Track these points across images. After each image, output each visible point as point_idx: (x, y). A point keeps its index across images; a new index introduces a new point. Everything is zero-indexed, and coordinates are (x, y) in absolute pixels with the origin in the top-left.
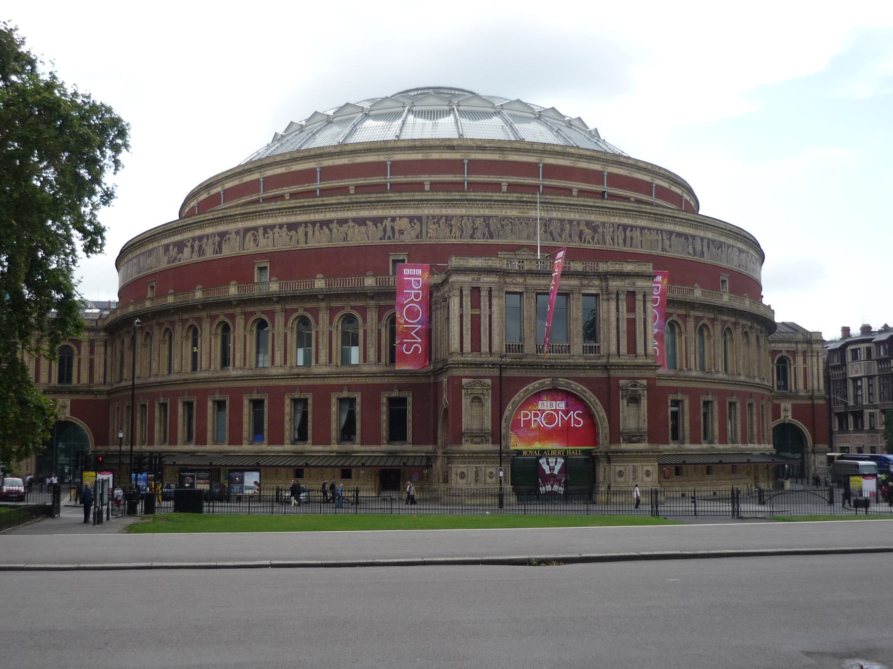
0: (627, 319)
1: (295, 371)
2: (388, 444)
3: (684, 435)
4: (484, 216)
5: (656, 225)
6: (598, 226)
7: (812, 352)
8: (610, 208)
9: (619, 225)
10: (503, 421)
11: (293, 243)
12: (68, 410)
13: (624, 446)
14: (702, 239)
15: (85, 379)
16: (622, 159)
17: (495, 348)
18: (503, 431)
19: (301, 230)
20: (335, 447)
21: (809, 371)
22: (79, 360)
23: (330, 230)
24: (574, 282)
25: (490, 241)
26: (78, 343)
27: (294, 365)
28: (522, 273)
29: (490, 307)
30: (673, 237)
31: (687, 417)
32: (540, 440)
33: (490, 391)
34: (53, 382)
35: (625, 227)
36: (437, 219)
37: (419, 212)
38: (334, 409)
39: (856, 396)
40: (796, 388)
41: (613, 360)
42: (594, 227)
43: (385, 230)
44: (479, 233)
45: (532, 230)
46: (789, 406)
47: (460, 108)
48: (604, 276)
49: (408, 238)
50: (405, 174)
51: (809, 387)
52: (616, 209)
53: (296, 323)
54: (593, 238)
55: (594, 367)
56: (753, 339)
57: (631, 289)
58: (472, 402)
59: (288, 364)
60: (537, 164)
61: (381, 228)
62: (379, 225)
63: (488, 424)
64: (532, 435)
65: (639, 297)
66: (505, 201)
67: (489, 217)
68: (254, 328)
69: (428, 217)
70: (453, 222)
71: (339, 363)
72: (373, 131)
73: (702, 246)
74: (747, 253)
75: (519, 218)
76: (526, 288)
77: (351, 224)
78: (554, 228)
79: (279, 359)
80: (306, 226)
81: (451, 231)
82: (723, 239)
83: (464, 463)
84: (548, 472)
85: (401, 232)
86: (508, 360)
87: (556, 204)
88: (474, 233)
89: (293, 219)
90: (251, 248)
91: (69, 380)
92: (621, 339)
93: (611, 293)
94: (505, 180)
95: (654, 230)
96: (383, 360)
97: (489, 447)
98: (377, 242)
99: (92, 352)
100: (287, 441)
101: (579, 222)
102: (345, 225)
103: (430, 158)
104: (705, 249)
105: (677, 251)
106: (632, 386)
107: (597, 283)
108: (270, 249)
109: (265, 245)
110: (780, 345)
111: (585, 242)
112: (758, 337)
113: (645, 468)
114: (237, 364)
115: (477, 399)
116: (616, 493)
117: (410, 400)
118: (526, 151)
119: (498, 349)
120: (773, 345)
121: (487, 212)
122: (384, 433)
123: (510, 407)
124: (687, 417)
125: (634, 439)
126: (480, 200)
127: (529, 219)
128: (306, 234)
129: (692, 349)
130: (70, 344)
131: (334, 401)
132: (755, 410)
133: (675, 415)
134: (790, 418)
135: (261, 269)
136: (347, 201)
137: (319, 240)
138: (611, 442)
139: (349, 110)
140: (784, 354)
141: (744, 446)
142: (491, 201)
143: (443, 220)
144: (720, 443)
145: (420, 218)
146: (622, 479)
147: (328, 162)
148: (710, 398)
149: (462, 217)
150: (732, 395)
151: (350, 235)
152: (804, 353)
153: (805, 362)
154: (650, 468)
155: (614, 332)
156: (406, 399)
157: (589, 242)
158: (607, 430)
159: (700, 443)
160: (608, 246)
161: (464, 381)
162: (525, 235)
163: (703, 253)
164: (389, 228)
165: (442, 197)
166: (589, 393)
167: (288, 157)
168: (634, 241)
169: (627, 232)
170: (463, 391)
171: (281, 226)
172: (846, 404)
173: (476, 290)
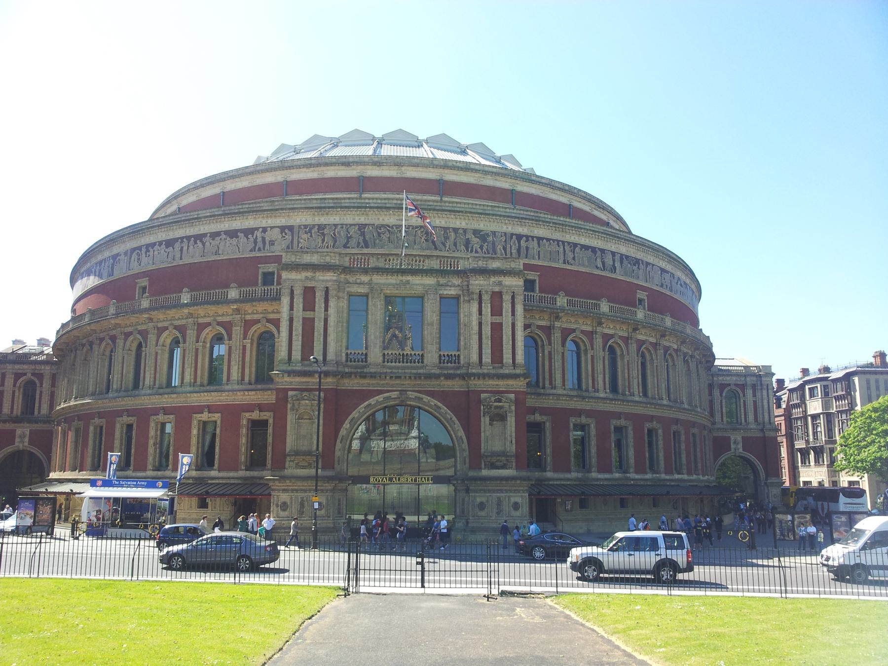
0: (492, 323)
2: (246, 470)
3: (590, 462)
5: (557, 236)
7: (761, 385)
8: (500, 216)
9: (512, 235)
11: (170, 259)
12: (27, 440)
13: (485, 472)
14: (613, 254)
15: (45, 410)
16: (533, 178)
17: (331, 356)
18: (338, 453)
19: (177, 246)
21: (759, 404)
22: (41, 392)
23: (204, 244)
24: (430, 281)
25: (365, 251)
26: (40, 376)
28: (365, 271)
29: (326, 309)
30: (577, 249)
31: (593, 443)
34: (15, 413)
35: (519, 237)
36: (308, 229)
37: (291, 222)
38: (195, 432)
39: (815, 433)
40: (746, 421)
42: (484, 235)
43: (255, 242)
44: (353, 242)
46: (739, 439)
49: (277, 250)
51: (760, 419)
52: (508, 217)
54: (481, 247)
56: (680, 362)
57: (497, 289)
58: (300, 418)
59: (157, 386)
60: (436, 180)
61: (252, 239)
62: (250, 236)
65: (507, 298)
66: (381, 208)
71: (206, 382)
73: (614, 261)
74: (673, 275)
76: (372, 289)
77: (223, 236)
80: (182, 242)
81: (323, 240)
82: (640, 255)
85: (272, 243)
86: (347, 370)
88: (348, 242)
89: (171, 235)
90: (136, 269)
91: (33, 413)
93: (473, 293)
95: (554, 241)
96: (247, 378)
97: (313, 472)
99: (53, 385)
100: (150, 467)
101: (465, 231)
102: (218, 238)
103: (326, 176)
104: (617, 264)
106: (496, 401)
107: (457, 281)
109: (147, 264)
110: (728, 378)
112: (686, 362)
113: (513, 500)
114: (115, 387)
116: (473, 531)
117: (271, 421)
118: (425, 166)
119: (334, 358)
120: (720, 378)
121: (362, 220)
122: (243, 459)
124: (593, 443)
126: (354, 207)
128: (181, 250)
129: (599, 367)
130: (32, 378)
132: (683, 438)
134: (741, 450)
135: (144, 288)
137: (193, 256)
138: (471, 468)
140: (733, 387)
141: (668, 477)
144: (636, 472)
145: (291, 228)
146: (483, 513)
147: (230, 186)
148: (622, 422)
149: (336, 225)
150: (652, 421)
151: (221, 248)
152: (754, 387)
153: (754, 395)
154: (519, 500)
155: (476, 338)
156: (267, 421)
157: (476, 252)
158: (466, 454)
161: (290, 393)
163: (615, 268)
164: (259, 240)
166: (444, 409)
168: (530, 251)
169: (522, 242)
170: (289, 406)
171: (160, 243)
172: (807, 442)
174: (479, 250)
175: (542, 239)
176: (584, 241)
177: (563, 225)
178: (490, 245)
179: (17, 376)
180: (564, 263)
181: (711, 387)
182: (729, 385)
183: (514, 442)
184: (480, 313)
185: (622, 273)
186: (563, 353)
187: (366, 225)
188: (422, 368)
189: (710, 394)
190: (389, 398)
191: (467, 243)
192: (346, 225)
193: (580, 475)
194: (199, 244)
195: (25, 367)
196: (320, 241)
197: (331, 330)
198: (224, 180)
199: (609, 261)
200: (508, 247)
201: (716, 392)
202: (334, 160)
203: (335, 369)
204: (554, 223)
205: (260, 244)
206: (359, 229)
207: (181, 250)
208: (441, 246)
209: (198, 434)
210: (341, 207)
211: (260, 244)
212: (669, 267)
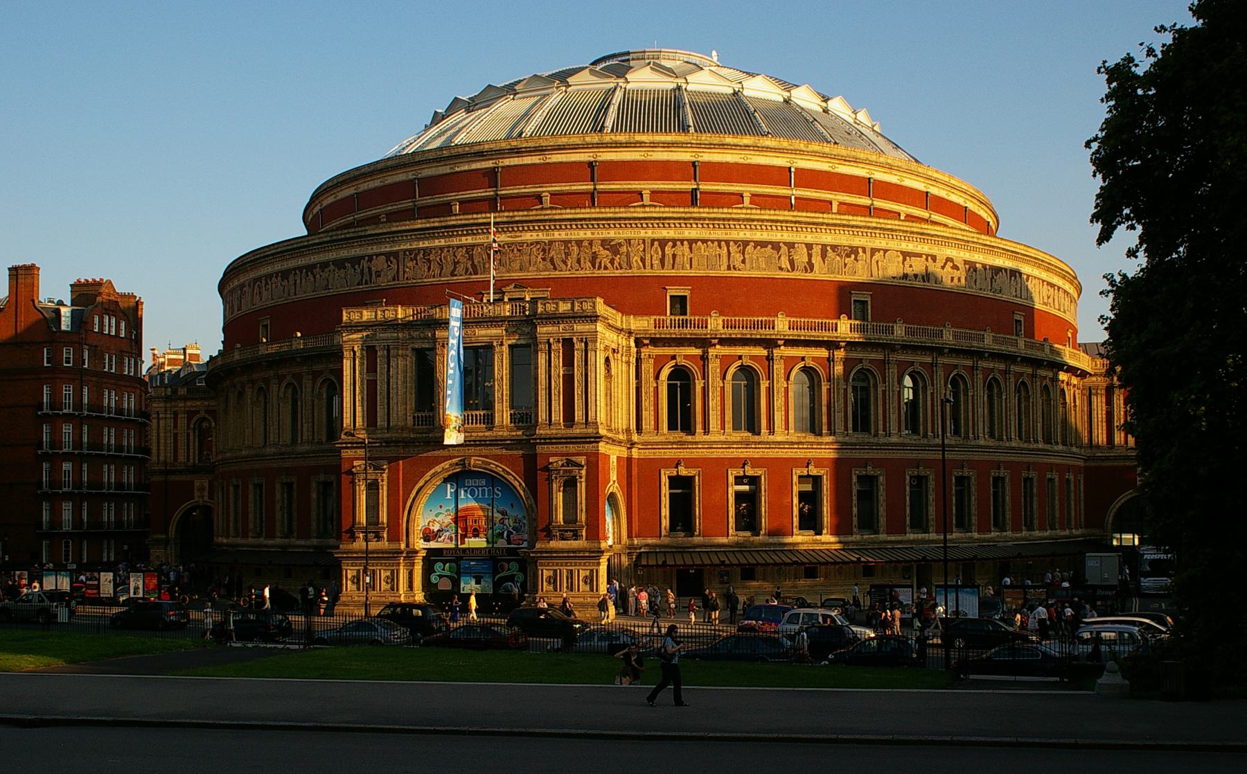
1: (283, 449)
6: (620, 245)
9: (653, 241)
13: (554, 544)
14: (809, 246)
19: (291, 278)
20: (315, 541)
30: (749, 248)
35: (663, 243)
38: (314, 495)
43: (362, 273)
44: (461, 268)
45: (526, 258)
49: (383, 282)
53: (290, 390)
54: (612, 262)
57: (567, 336)
60: (590, 164)
65: (579, 346)
67: (473, 246)
68: (262, 399)
71: (324, 439)
73: (810, 256)
74: (934, 258)
75: (509, 245)
77: (332, 267)
79: (273, 438)
81: (429, 268)
82: (858, 241)
88: (454, 270)
90: (259, 305)
94: (546, 190)
95: (713, 241)
98: (355, 288)
100: (278, 534)
101: (591, 243)
104: (816, 260)
105: (757, 268)
108: (270, 303)
111: (599, 268)
115: (373, 487)
131: (314, 485)
133: (739, 496)
145: (395, 254)
147: (365, 186)
149: (442, 248)
157: (606, 268)
160: (635, 272)
163: (810, 266)
164: (366, 270)
168: (678, 259)
171: (277, 274)
175: (696, 241)
178: (624, 258)
189: (1109, 402)
191: (594, 257)
194: (311, 277)
198: (356, 178)
199: (801, 257)
200: (648, 257)
204: (710, 219)
205: (367, 277)
206: (467, 252)
209: (318, 498)
211: (367, 277)
212: (924, 248)
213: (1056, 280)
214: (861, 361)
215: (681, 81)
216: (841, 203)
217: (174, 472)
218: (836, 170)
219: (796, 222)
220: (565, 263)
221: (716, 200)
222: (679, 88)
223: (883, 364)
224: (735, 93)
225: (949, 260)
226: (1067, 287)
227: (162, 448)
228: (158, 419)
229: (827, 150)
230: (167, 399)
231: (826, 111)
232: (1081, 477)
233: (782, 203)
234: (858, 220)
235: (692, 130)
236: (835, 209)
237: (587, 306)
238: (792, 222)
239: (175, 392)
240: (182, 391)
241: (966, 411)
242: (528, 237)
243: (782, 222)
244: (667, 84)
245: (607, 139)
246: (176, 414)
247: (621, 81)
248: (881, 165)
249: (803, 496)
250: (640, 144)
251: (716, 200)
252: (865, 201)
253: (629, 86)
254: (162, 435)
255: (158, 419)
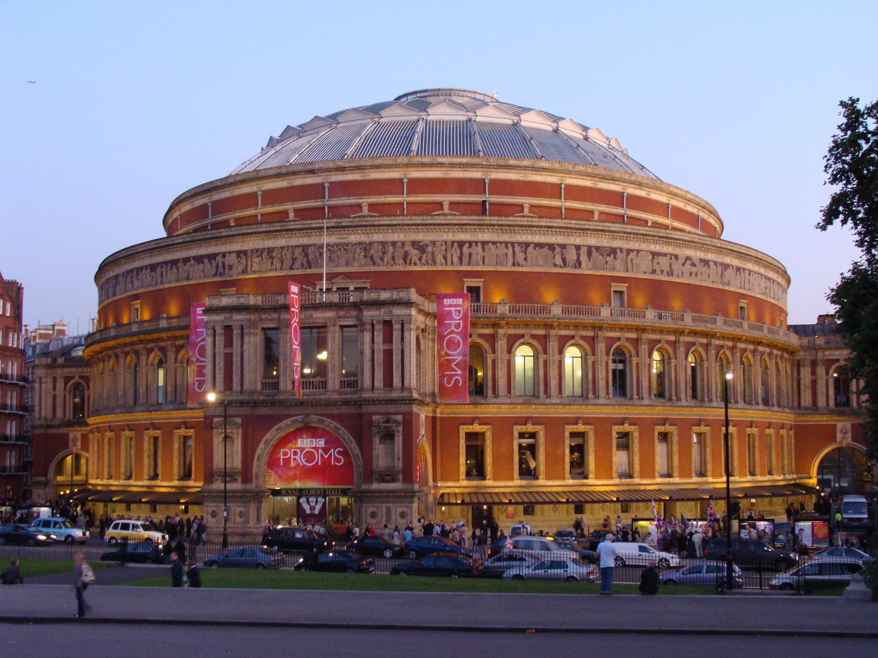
0: (384, 350)
4: (302, 246)
6: (427, 245)
8: (439, 225)
9: (453, 242)
10: (255, 461)
13: (376, 486)
14: (578, 247)
17: (246, 387)
18: (255, 470)
19: (159, 270)
23: (178, 269)
24: (330, 314)
25: (309, 271)
27: (155, 402)
30: (530, 249)
32: (300, 479)
33: (240, 430)
35: (461, 244)
36: (259, 252)
38: (176, 445)
41: (366, 395)
43: (217, 267)
44: (298, 264)
45: (351, 256)
47: (382, 120)
48: (358, 306)
50: (273, 204)
54: (420, 259)
55: (346, 403)
57: (387, 318)
60: (401, 180)
61: (214, 265)
63: (237, 462)
64: (291, 473)
65: (397, 326)
69: (252, 250)
70: (274, 254)
72: (295, 153)
73: (578, 255)
75: (337, 245)
76: (279, 323)
77: (192, 262)
78: (375, 252)
80: (162, 267)
81: (272, 263)
82: (616, 244)
83: (215, 502)
84: (308, 511)
85: (230, 267)
86: (261, 398)
87: (374, 226)
92: (376, 372)
94: (365, 201)
95: (501, 243)
101: (403, 243)
102: (188, 264)
104: (584, 258)
106: (384, 422)
107: (354, 313)
110: (837, 353)
111: (410, 264)
113: (400, 510)
120: (827, 353)
121: (305, 241)
123: (262, 445)
125: (387, 478)
127: (347, 244)
128: (162, 275)
130: (80, 381)
132: (675, 439)
134: (850, 440)
136: (189, 239)
139: (291, 132)
142: (307, 229)
143: (265, 253)
145: (245, 252)
148: (580, 428)
149: (282, 248)
150: (623, 424)
158: (361, 469)
159: (563, 478)
161: (216, 420)
162: (343, 261)
163: (579, 263)
164: (220, 265)
165: (264, 229)
166: (343, 431)
167: (192, 193)
168: (473, 257)
169: (466, 250)
171: (146, 267)
173: (228, 329)
174: (418, 262)
175: (487, 243)
176: (537, 239)
177: (510, 226)
178: (430, 256)
179: (67, 379)
180: (514, 265)
181: (814, 364)
182: (838, 360)
183: (401, 458)
184: (373, 342)
185: (590, 266)
186: (509, 362)
187: (309, 245)
188: (324, 393)
189: (814, 373)
190: (296, 421)
192: (292, 247)
193: (524, 483)
194: (175, 270)
195: (73, 370)
196: (269, 263)
197: (246, 364)
199: (571, 256)
201: (821, 371)
202: (301, 168)
203: (249, 398)
204: (499, 225)
205: (221, 270)
206: (303, 250)
207: (162, 275)
208: (380, 262)
209: (180, 448)
210: (286, 230)
211: (221, 270)
212: (669, 249)
213: (772, 275)
214: (619, 339)
215: (471, 114)
216: (601, 213)
217: (52, 427)
218: (597, 186)
219: (567, 228)
220: (382, 259)
221: (500, 209)
222: (470, 120)
223: (636, 342)
224: (515, 124)
225: (688, 258)
226: (780, 280)
227: (43, 406)
228: (41, 383)
229: (590, 170)
230: (49, 366)
231: (586, 138)
232: (792, 432)
233: (555, 212)
234: (616, 227)
235: (481, 154)
236: (596, 217)
237: (402, 295)
238: (564, 228)
239: (54, 361)
240: (61, 361)
241: (702, 380)
242: (353, 238)
243: (556, 227)
244: (461, 117)
245: (415, 160)
246: (55, 380)
247: (423, 115)
248: (633, 183)
249: (572, 450)
250: (442, 165)
251: (500, 209)
252: (619, 211)
253: (430, 118)
254: (43, 396)
255: (41, 383)
